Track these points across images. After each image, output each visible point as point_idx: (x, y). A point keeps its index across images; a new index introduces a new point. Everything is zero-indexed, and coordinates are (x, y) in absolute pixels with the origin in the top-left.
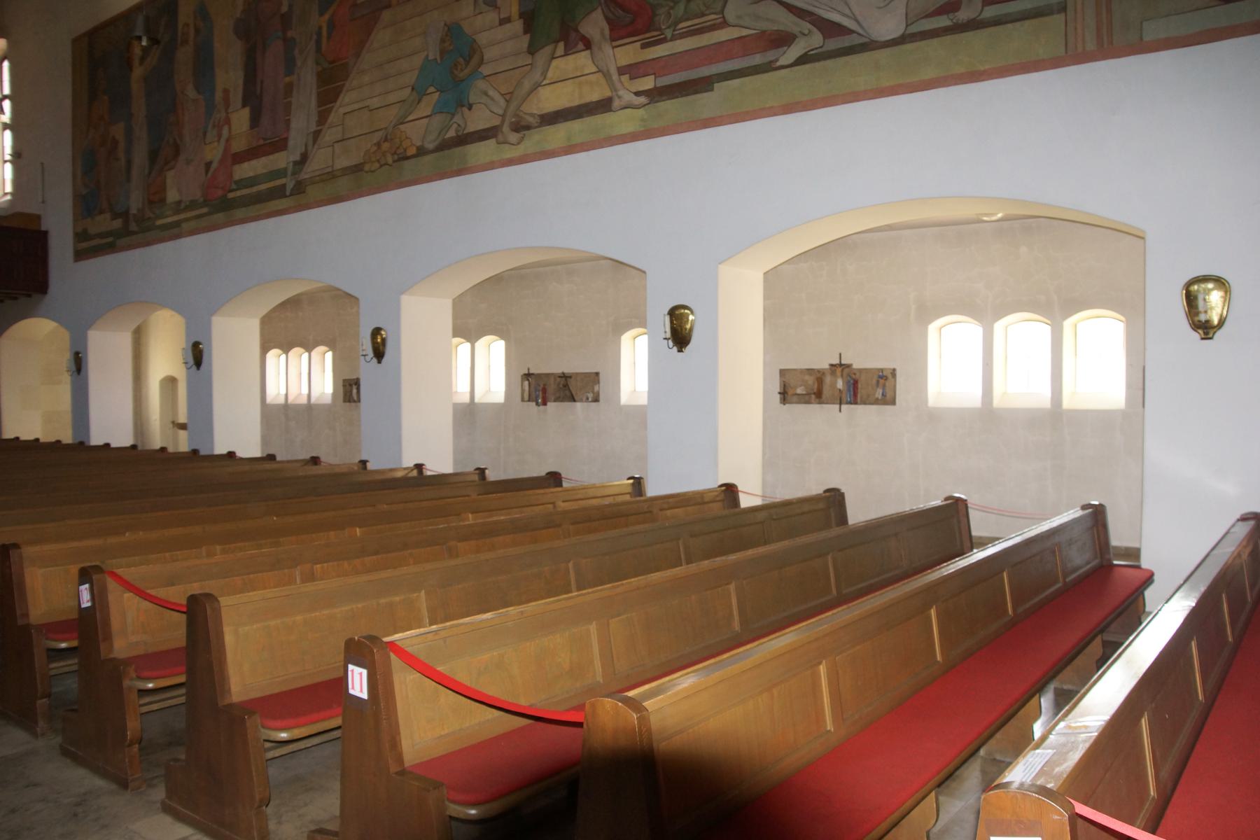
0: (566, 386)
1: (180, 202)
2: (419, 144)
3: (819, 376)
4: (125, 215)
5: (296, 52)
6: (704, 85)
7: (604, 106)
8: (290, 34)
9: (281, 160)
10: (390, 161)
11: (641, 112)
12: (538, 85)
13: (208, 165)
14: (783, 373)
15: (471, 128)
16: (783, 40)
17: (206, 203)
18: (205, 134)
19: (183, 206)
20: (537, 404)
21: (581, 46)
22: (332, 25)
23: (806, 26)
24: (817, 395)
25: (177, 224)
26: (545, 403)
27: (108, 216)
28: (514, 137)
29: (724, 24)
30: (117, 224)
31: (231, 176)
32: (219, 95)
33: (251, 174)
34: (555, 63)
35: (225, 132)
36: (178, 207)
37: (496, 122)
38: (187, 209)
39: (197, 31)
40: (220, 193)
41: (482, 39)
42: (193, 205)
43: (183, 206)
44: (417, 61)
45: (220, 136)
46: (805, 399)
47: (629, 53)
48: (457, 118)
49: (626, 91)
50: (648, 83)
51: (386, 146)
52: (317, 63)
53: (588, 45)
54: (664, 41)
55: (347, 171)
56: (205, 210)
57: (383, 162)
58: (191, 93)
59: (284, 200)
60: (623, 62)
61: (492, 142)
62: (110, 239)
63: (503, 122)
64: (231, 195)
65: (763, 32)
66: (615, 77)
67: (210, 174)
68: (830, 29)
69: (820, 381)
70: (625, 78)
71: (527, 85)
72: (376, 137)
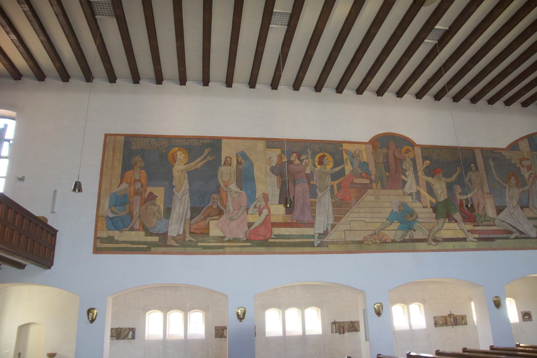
0: (353, 326)
1: (224, 237)
2: (393, 238)
3: (445, 318)
4: (164, 236)
5: (317, 190)
6: (492, 239)
7: (464, 240)
8: (312, 182)
9: (309, 231)
10: (378, 242)
11: (476, 243)
12: (440, 230)
13: (250, 225)
14: (434, 318)
15: (416, 237)
16: (511, 233)
17: (247, 240)
18: (247, 209)
19: (226, 239)
20: (340, 333)
21: (454, 221)
22: (339, 186)
23: (515, 230)
24: (446, 324)
25: (223, 247)
26: (344, 333)
27: (142, 233)
28: (434, 243)
29: (495, 225)
30: (156, 239)
31: (272, 232)
32: (259, 194)
33: (287, 234)
34: (445, 224)
35: (265, 212)
36: (221, 239)
37: (427, 237)
38: (229, 241)
39: (239, 163)
40: (262, 238)
41: (417, 210)
42: (235, 240)
43: (226, 239)
44: (389, 210)
45: (260, 214)
46: (442, 325)
47: (469, 227)
48: (409, 233)
49: (471, 237)
50: (477, 236)
51: (375, 236)
52: (332, 198)
53: (456, 221)
54: (479, 226)
55: (353, 242)
56: (249, 244)
57: (374, 241)
58: (233, 187)
59: (313, 248)
60: (469, 229)
61: (425, 243)
62: (146, 246)
63: (429, 237)
64: (270, 240)
65: (505, 230)
66: (466, 232)
67: (251, 228)
68: (521, 232)
69: (446, 320)
70: (470, 233)
71: (436, 228)
72: (370, 233)
